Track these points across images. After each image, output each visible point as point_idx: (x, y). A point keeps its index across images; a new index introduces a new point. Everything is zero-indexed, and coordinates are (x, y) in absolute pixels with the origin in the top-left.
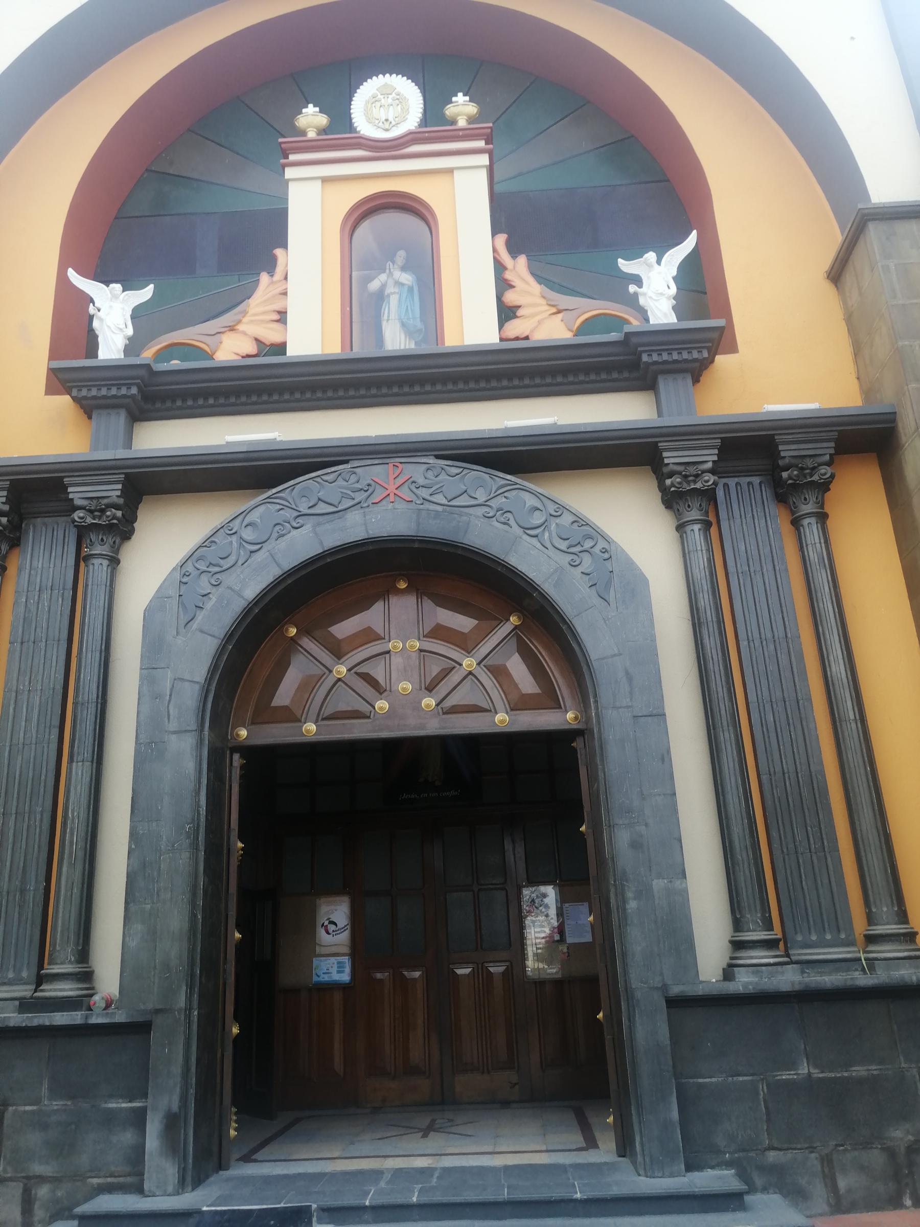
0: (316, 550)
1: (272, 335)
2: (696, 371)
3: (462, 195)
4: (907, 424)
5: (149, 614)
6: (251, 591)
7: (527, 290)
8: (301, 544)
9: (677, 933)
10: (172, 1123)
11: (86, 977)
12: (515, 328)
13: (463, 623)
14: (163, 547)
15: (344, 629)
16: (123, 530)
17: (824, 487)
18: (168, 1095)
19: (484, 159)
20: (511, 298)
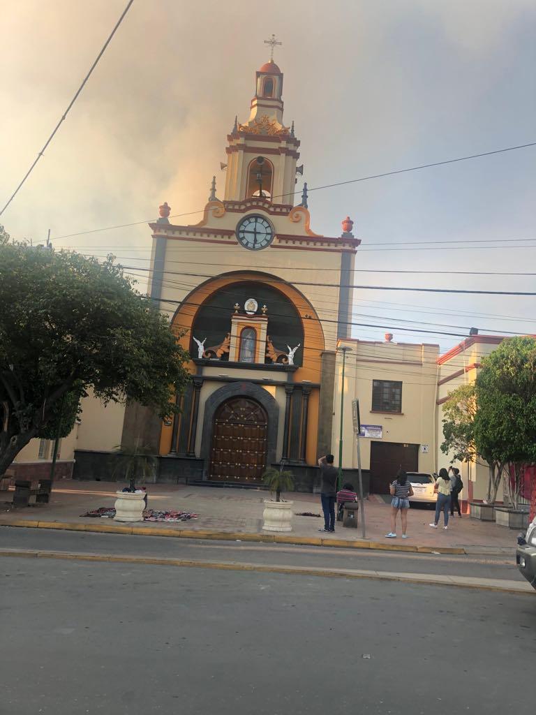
0: (230, 396)
1: (227, 351)
2: (294, 372)
3: (262, 328)
4: (321, 387)
5: (206, 403)
6: (221, 401)
7: (271, 348)
8: (229, 394)
9: (274, 455)
10: (206, 474)
11: (194, 453)
12: (268, 355)
13: (252, 407)
14: (207, 391)
15: (233, 406)
16: (201, 386)
17: (309, 395)
18: (206, 469)
19: (267, 323)
20: (268, 349)
